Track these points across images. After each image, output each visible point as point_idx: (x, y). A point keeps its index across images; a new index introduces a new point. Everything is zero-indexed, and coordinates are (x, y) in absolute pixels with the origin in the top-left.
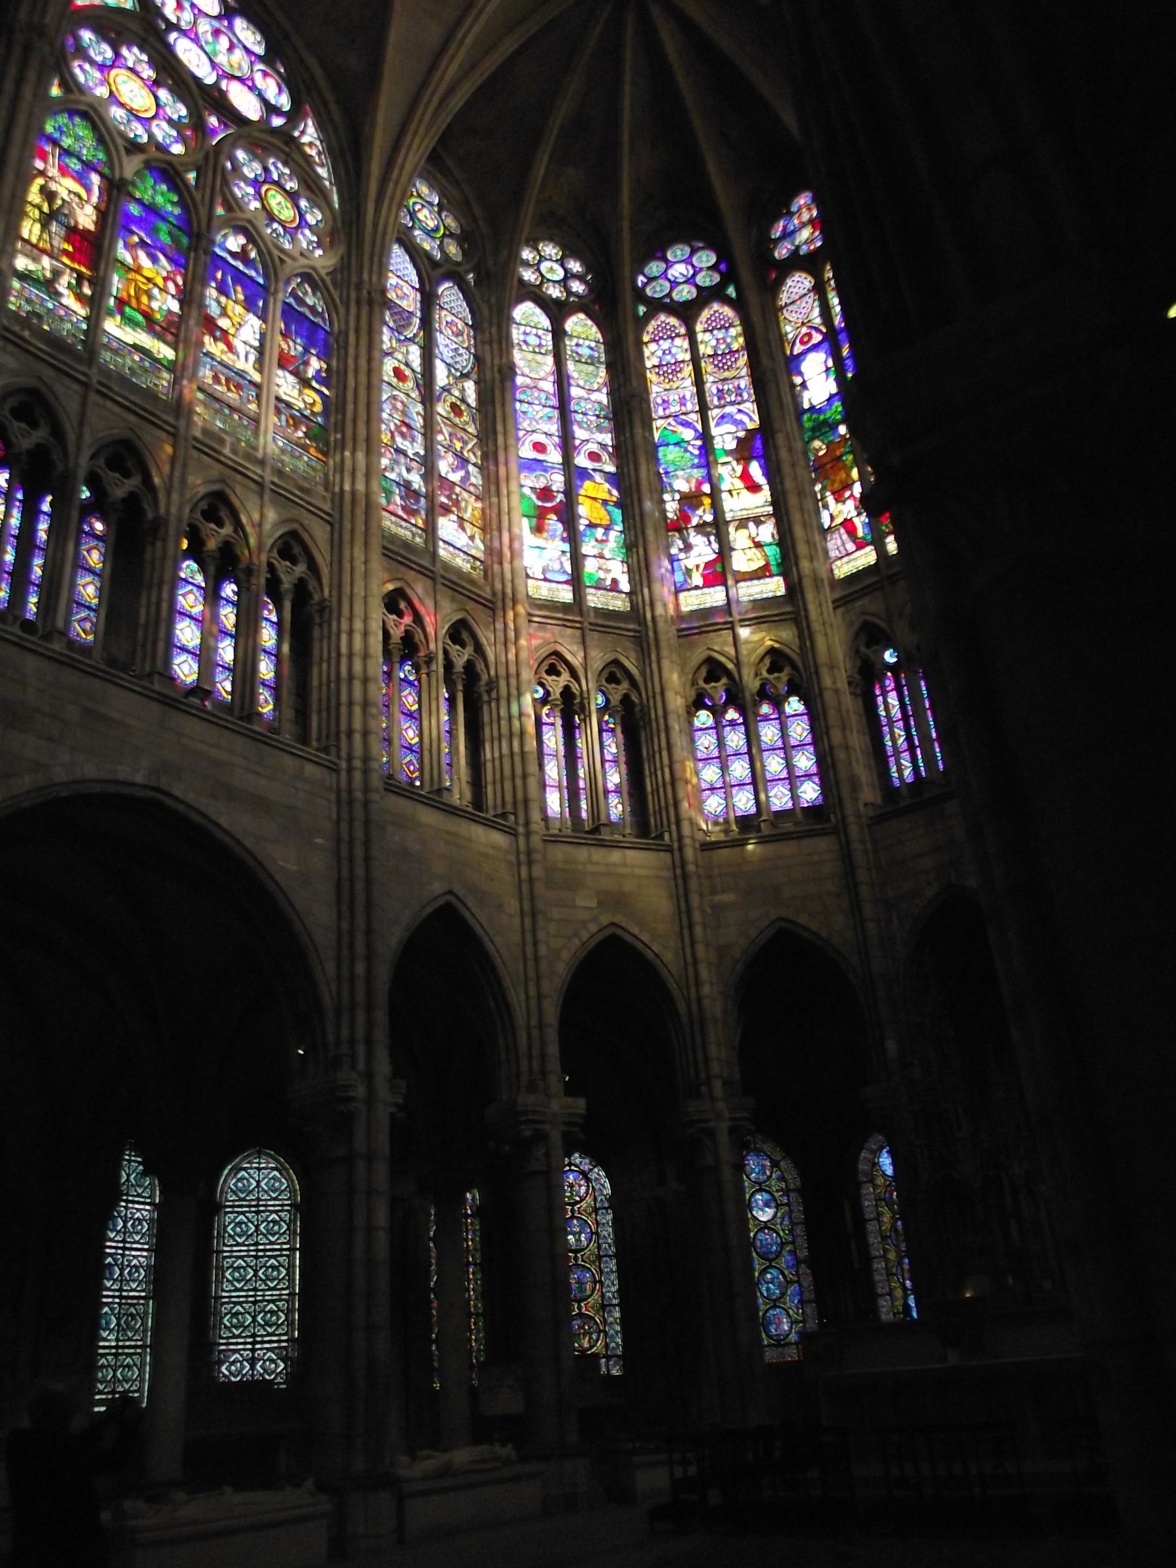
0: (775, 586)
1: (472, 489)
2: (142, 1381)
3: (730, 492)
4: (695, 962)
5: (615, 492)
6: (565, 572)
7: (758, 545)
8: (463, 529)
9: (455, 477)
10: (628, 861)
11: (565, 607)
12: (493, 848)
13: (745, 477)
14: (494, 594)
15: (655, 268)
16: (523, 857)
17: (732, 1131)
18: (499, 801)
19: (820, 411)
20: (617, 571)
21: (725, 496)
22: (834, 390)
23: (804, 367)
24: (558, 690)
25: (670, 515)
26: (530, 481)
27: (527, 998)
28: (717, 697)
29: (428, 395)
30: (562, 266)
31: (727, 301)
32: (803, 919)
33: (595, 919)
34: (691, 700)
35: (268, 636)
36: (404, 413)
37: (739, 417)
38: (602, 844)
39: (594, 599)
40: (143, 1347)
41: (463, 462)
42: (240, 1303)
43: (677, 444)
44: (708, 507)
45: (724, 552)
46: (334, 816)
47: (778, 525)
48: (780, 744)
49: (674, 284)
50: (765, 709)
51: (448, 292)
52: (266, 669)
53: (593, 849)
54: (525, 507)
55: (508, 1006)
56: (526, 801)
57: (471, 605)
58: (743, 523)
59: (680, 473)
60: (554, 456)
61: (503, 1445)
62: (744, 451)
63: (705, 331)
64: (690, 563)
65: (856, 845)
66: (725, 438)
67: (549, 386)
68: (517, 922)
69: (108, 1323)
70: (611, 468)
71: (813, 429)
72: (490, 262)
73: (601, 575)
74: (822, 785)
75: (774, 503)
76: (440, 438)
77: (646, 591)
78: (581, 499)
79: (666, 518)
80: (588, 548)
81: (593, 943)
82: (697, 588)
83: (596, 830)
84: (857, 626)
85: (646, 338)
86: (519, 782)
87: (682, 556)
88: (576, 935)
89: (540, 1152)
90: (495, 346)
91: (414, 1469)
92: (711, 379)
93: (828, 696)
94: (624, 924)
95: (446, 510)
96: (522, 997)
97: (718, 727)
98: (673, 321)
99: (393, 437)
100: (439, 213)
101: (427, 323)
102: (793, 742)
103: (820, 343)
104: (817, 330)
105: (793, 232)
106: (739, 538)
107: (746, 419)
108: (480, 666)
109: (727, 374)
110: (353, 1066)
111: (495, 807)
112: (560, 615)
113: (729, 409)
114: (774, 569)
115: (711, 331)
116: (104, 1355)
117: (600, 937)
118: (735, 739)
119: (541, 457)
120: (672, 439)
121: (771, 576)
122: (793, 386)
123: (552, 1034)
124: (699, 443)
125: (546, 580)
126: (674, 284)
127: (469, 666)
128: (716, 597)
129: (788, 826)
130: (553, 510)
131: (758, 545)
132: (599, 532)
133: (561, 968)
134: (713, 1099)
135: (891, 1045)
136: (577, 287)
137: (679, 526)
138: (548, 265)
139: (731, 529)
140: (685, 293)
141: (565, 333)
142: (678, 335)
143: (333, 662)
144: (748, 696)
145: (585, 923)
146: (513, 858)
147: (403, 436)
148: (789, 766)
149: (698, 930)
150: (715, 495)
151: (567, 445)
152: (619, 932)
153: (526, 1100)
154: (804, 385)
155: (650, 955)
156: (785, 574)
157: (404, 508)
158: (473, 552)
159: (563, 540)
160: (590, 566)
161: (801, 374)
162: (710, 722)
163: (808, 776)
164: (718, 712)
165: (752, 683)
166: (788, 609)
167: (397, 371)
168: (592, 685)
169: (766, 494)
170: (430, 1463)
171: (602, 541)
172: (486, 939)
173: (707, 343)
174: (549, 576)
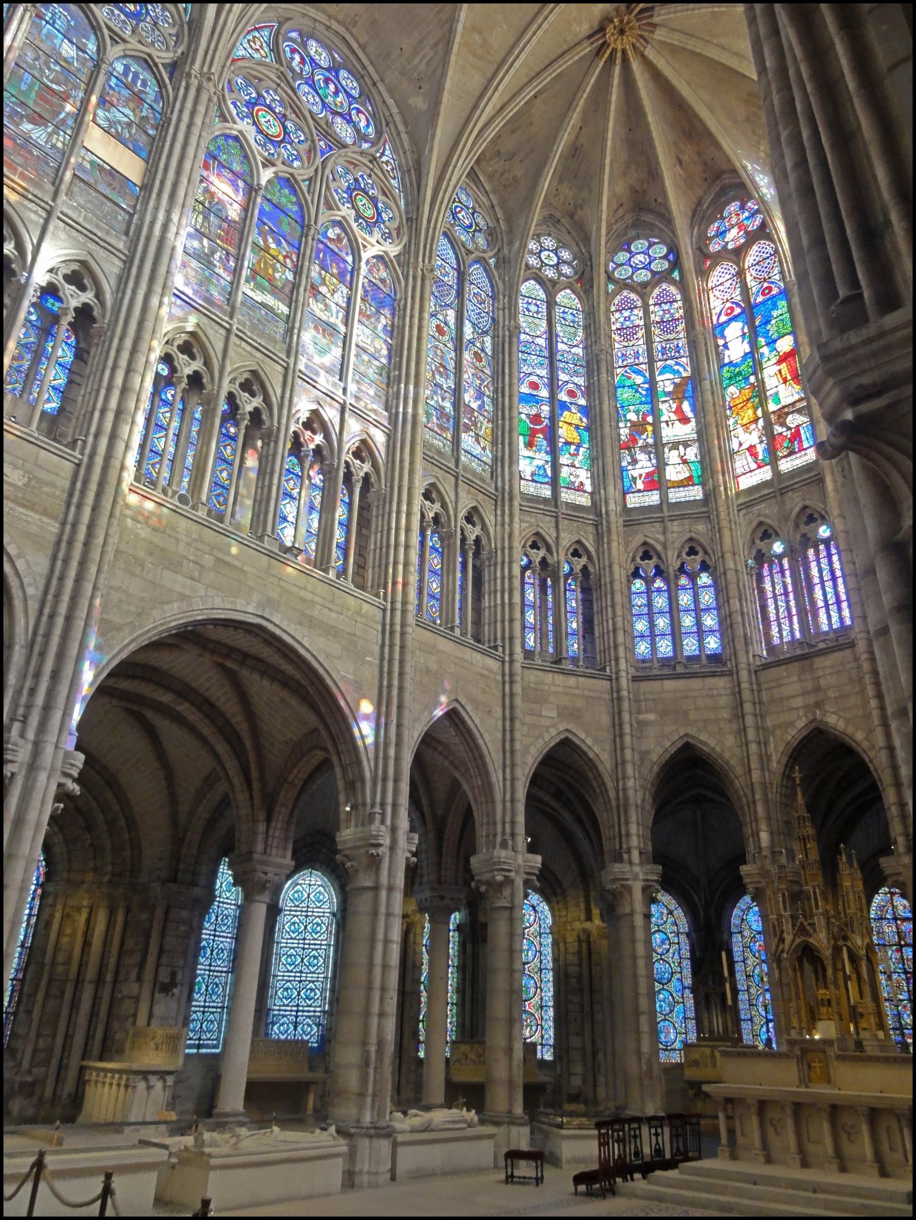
0: (696, 493)
2: (220, 1032)
3: (667, 422)
4: (624, 762)
5: (585, 420)
6: (546, 476)
7: (685, 462)
9: (474, 405)
11: (545, 501)
13: (679, 411)
14: (496, 489)
15: (622, 257)
16: (507, 678)
17: (645, 889)
18: (492, 638)
19: (736, 365)
20: (584, 477)
21: (663, 425)
22: (748, 350)
23: (727, 332)
24: (538, 560)
25: (623, 438)
26: (526, 410)
27: (504, 779)
28: (649, 570)
29: (459, 348)
30: (556, 254)
31: (673, 282)
32: (703, 737)
34: (630, 572)
35: (340, 513)
36: (442, 357)
37: (676, 368)
38: (564, 672)
39: (566, 496)
40: (222, 1008)
41: (480, 395)
42: (290, 981)
43: (630, 387)
44: (650, 433)
45: (661, 465)
46: (380, 642)
47: (700, 448)
48: (692, 607)
49: (635, 269)
50: (683, 581)
51: (476, 272)
52: (338, 535)
53: (556, 675)
54: (522, 428)
55: (490, 784)
56: (511, 638)
58: (675, 446)
59: (632, 408)
60: (544, 393)
61: (468, 1110)
62: (678, 394)
63: (655, 305)
64: (635, 473)
65: (745, 686)
66: (665, 382)
67: (542, 342)
68: (500, 723)
69: (200, 989)
70: (582, 402)
71: (730, 378)
72: (506, 251)
73: (572, 479)
74: (722, 638)
75: (699, 432)
76: (466, 376)
77: (602, 491)
78: (561, 424)
79: (620, 440)
80: (564, 459)
81: (552, 744)
82: (639, 491)
83: (558, 661)
84: (754, 524)
85: (613, 308)
86: (507, 623)
87: (630, 467)
88: (541, 736)
89: (507, 892)
90: (507, 311)
91: (403, 1123)
92: (658, 339)
93: (731, 575)
95: (468, 429)
96: (501, 778)
97: (649, 592)
98: (633, 296)
99: (433, 375)
100: (473, 214)
101: (460, 294)
102: (702, 607)
103: (739, 314)
104: (738, 305)
105: (724, 232)
106: (672, 457)
107: (681, 370)
108: (484, 541)
109: (669, 336)
110: (383, 822)
111: (489, 641)
113: (669, 362)
114: (696, 480)
115: (660, 305)
116: (195, 1012)
118: (660, 602)
119: (535, 393)
120: (628, 383)
121: (693, 485)
122: (717, 346)
123: (521, 807)
124: (646, 386)
125: (533, 481)
126: (635, 269)
127: (478, 541)
128: (653, 498)
129: (696, 668)
130: (542, 431)
131: (685, 462)
132: (573, 447)
134: (630, 863)
135: (764, 836)
136: (566, 270)
137: (629, 446)
138: (547, 253)
139: (666, 450)
140: (643, 276)
141: (556, 303)
142: (636, 307)
143: (385, 533)
144: (671, 571)
145: (547, 728)
146: (499, 678)
147: (441, 375)
148: (699, 623)
149: (627, 739)
150: (656, 425)
151: (553, 385)
152: (571, 737)
153: (502, 854)
154: (726, 346)
155: (591, 755)
156: (703, 484)
158: (484, 459)
159: (547, 453)
160: (565, 472)
161: (723, 337)
162: (643, 588)
163: (712, 631)
164: (649, 582)
165: (673, 563)
166: (704, 510)
167: (438, 326)
168: (562, 558)
169: (693, 423)
170: (417, 1118)
172: (478, 735)
173: (656, 313)
174: (535, 478)
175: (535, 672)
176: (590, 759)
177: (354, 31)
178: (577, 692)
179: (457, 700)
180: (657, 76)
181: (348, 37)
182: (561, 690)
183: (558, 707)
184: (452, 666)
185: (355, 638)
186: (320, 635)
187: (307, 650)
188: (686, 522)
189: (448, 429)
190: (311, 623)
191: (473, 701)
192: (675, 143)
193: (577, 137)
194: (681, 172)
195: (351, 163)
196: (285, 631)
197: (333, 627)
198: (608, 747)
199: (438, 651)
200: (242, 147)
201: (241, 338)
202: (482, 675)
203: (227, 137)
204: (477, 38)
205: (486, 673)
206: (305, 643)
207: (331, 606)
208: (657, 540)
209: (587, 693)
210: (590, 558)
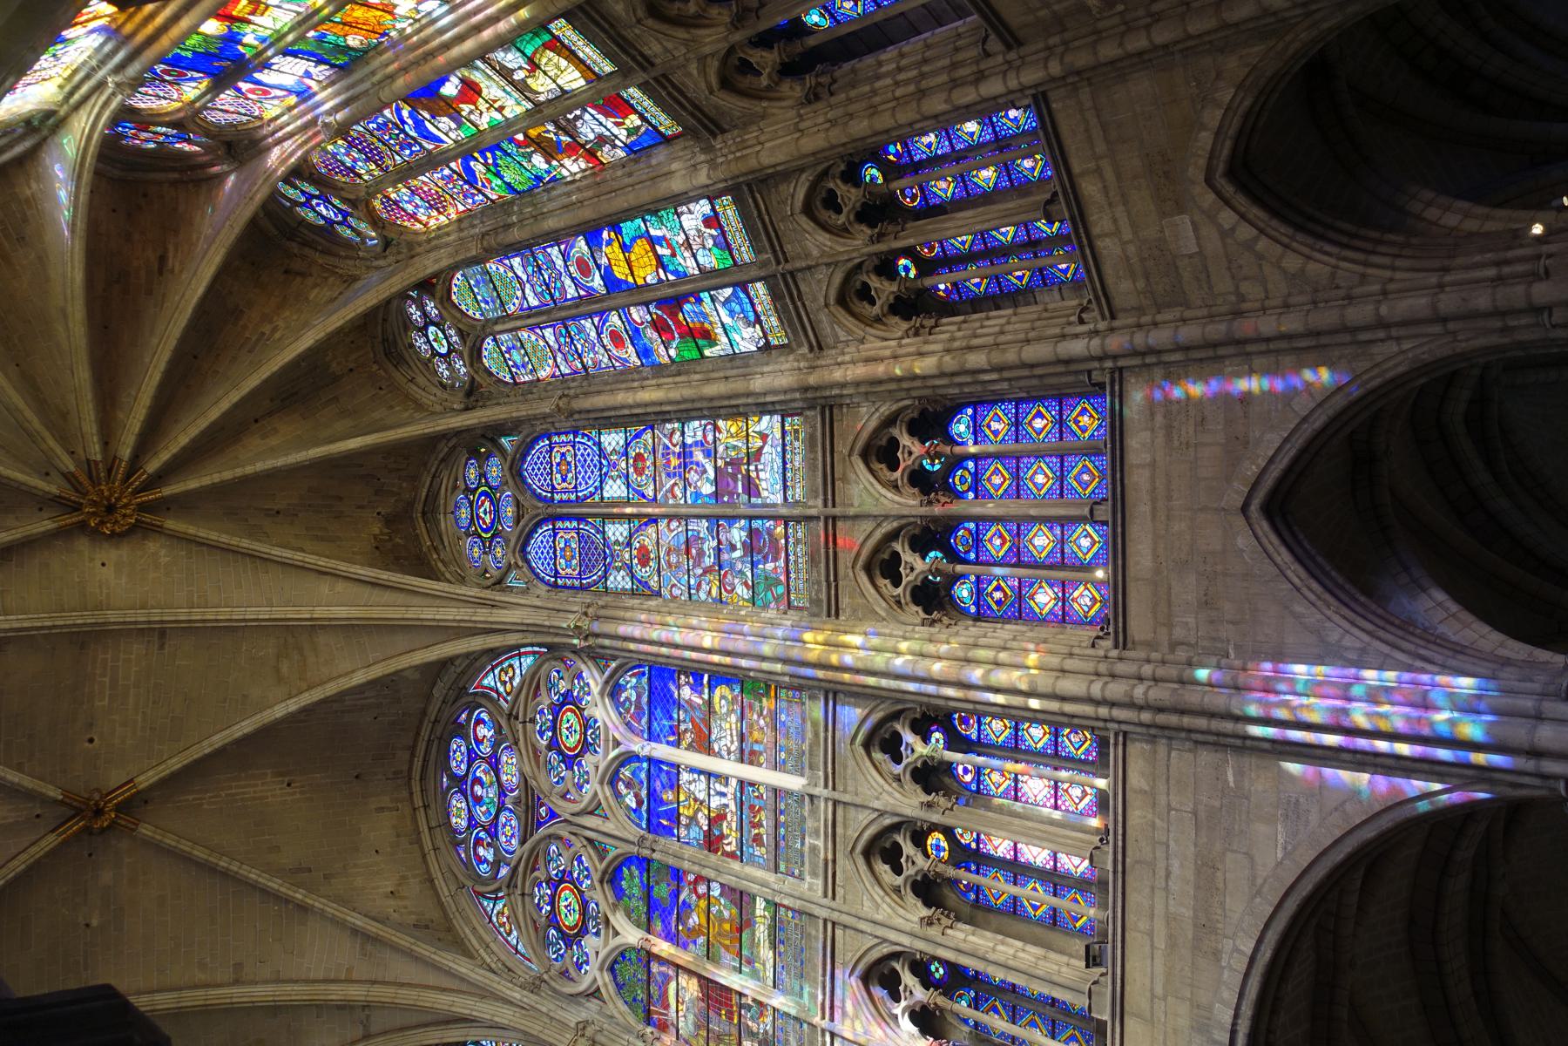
1: (710, 438)
6: (734, 294)
10: (1092, 165)
12: (1152, 414)
14: (811, 408)
33: (1212, 218)
53: (1096, 231)
57: (842, 448)
73: (710, 243)
81: (1255, 212)
88: (1249, 246)
94: (1202, 162)
95: (751, 488)
96: (1393, 348)
117: (1241, 201)
121: (557, 38)
125: (758, 320)
130: (674, 316)
132: (660, 250)
133: (1317, 269)
145: (1225, 234)
152: (1221, 168)
157: (775, 560)
159: (699, 301)
160: (711, 259)
171: (670, 246)
172: (1308, 430)
174: (752, 318)
175: (1110, 281)
177: (405, 768)
179: (1244, 509)
180: (108, 397)
181: (416, 775)
182: (1120, 211)
184: (1177, 527)
185: (1202, 815)
186: (1223, 904)
187: (1260, 941)
188: (628, 34)
189: (770, 532)
190: (1206, 928)
192: (150, 293)
193: (270, 414)
194: (171, 248)
195: (537, 757)
196: (1241, 995)
197: (1198, 872)
199: (1157, 571)
200: (615, 962)
201: (832, 1007)
202: (1169, 428)
203: (619, 987)
204: (285, 669)
206: (1248, 947)
207: (1162, 873)
208: (703, 71)
209: (1101, 148)
210: (825, 174)
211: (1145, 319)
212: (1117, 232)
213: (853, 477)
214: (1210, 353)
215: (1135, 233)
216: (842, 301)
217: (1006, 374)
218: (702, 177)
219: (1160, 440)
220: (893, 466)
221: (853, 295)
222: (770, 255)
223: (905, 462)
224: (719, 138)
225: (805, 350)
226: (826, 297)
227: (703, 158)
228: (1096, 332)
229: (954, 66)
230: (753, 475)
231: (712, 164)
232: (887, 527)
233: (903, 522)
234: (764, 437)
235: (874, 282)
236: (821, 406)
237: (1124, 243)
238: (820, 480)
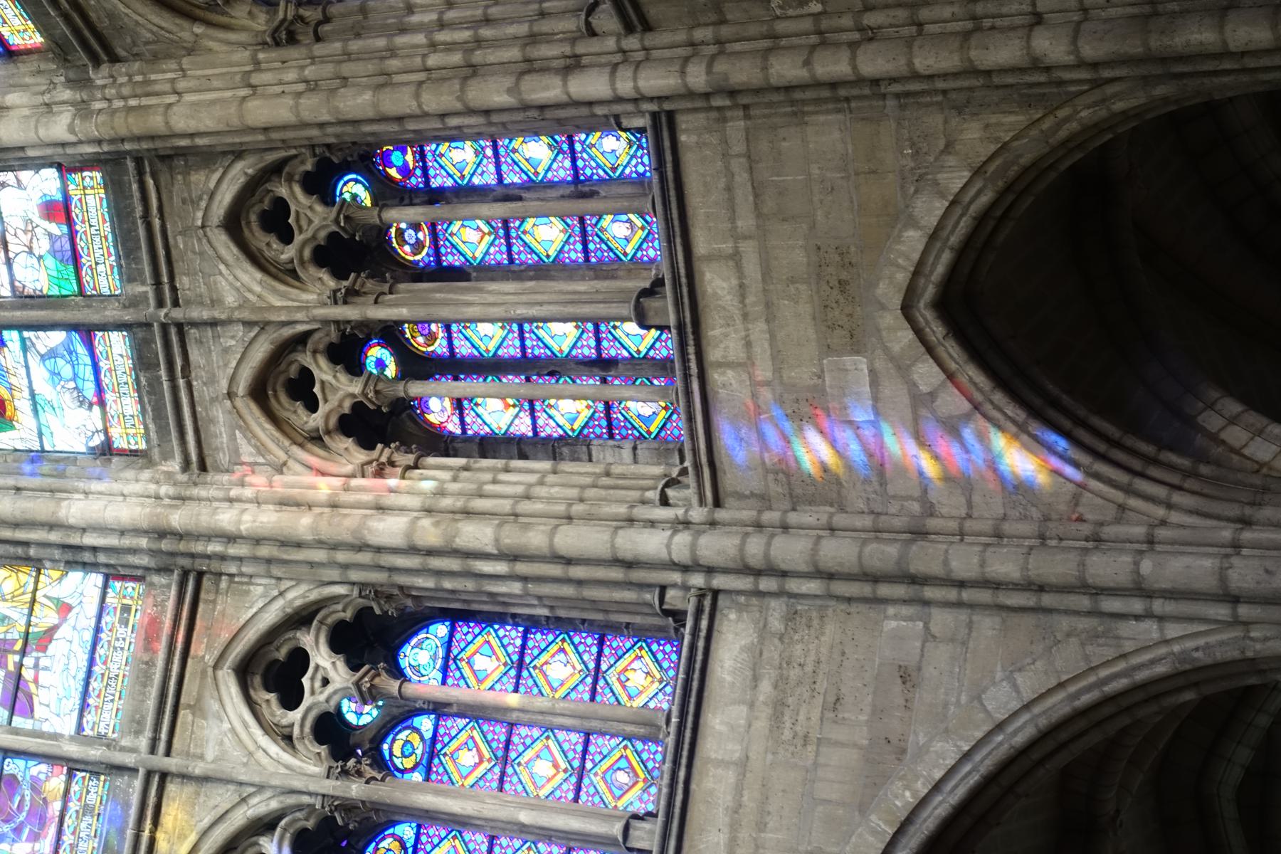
8: (53, 630)
10: (727, 247)
11: (143, 361)
12: (756, 679)
14: (164, 570)
16: (767, 584)
33: (903, 369)
53: (713, 355)
73: (42, 246)
81: (972, 374)
94: (902, 278)
96: (1150, 630)
112: (163, 373)
117: (952, 351)
125: (102, 403)
146: (777, 608)
152: (929, 292)
157: (34, 837)
172: (1003, 745)
174: (90, 390)
176: (1001, 195)
178: (752, 267)
182: (759, 330)
183: (828, 349)
189: (36, 786)
191: (874, 777)
198: (934, 120)
202: (779, 707)
205: (766, 687)
209: (746, 222)
210: (276, 170)
211: (770, 517)
212: (746, 365)
213: (215, 706)
214: (866, 589)
215: (777, 370)
216: (259, 392)
217: (522, 568)
218: (59, 127)
219: (761, 724)
220: (291, 699)
221: (280, 384)
222: (148, 289)
223: (314, 698)
224: (105, 69)
225: (174, 465)
226: (232, 379)
227: (67, 94)
228: (686, 524)
229: (533, 38)
230: (28, 674)
231: (82, 110)
232: (261, 806)
233: (291, 800)
234: (64, 609)
235: (323, 371)
236: (188, 570)
237: (755, 384)
238: (151, 704)
